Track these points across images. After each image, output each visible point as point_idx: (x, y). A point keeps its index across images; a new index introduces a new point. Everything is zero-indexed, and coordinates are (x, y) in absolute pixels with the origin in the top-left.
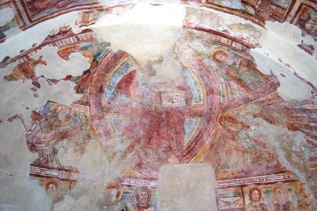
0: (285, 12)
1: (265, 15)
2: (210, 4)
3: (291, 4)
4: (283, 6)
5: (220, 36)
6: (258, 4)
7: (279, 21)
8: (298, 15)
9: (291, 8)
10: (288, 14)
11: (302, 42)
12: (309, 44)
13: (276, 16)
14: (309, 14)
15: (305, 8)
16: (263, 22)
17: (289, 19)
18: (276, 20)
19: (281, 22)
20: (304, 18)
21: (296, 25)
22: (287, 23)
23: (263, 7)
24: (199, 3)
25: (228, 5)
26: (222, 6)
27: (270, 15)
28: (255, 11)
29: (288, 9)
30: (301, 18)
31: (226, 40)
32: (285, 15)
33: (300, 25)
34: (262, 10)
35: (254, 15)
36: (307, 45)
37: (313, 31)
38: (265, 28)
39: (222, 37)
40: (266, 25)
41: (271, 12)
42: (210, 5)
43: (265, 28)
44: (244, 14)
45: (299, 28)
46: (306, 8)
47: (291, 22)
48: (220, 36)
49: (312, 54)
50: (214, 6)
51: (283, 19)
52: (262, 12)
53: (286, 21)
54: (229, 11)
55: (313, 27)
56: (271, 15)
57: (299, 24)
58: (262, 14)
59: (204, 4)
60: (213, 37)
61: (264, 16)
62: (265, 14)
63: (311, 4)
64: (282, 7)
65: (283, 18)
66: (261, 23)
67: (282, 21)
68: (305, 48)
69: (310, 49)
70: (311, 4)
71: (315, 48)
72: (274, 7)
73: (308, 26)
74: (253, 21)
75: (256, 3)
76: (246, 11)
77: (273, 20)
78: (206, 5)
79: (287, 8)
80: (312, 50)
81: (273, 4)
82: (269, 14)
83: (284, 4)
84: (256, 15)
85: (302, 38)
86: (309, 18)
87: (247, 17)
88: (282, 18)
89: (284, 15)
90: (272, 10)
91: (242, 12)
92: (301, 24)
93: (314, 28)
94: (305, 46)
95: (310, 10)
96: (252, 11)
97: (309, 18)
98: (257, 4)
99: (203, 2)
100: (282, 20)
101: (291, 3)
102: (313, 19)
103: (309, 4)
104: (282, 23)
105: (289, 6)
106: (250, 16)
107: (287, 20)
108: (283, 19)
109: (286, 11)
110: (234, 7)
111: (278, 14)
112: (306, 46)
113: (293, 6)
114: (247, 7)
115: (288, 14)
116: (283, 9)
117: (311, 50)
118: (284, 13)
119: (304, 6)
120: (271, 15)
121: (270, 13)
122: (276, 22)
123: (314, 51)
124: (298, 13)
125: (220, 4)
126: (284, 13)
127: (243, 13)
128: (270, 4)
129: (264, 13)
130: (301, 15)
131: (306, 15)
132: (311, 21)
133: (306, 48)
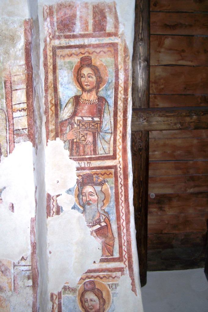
0: (91, 155)
1: (69, 133)
2: (51, 54)
3: (107, 156)
4: (99, 148)
5: (25, 87)
6: (84, 118)
7: (71, 155)
8: (95, 171)
9: (102, 158)
10: (91, 159)
11: (57, 196)
12: (59, 205)
13: (78, 147)
14: (104, 181)
15: (111, 173)
16: (57, 135)
17: (83, 164)
18: (71, 150)
19: (72, 157)
20: (94, 179)
21: (78, 176)
22: (75, 164)
23: (81, 125)
24: (51, 37)
25: (62, 79)
26: (57, 71)
27: (73, 140)
28: (68, 119)
29: (97, 156)
30: (93, 176)
31: (24, 98)
32: (87, 157)
33: (83, 180)
34: (76, 126)
35: (59, 120)
36: (57, 204)
37: (84, 198)
38: (47, 142)
39: (25, 91)
40: (54, 141)
41: (79, 140)
42: (50, 53)
43: (47, 142)
44: (54, 107)
45: (76, 181)
46: (112, 174)
47: (78, 169)
48: (27, 87)
49: (50, 216)
50: (51, 61)
51: (77, 157)
52: (72, 128)
53: (77, 162)
54: (49, 84)
55: (91, 195)
56: (75, 141)
57: (83, 178)
58: (68, 128)
59: (50, 44)
60: (19, 77)
61: (66, 133)
62: (71, 132)
63: (120, 176)
64: (95, 147)
65: (80, 157)
66: (52, 134)
67: (74, 158)
68: (51, 204)
69: (54, 210)
70: (120, 176)
71: (61, 214)
72: (90, 139)
73: (89, 189)
74: (47, 122)
75: (83, 115)
76: (61, 108)
77: (67, 147)
78: (48, 47)
79: (98, 154)
80: (54, 214)
81: (94, 137)
82: (74, 138)
83: (102, 149)
84: (62, 123)
85: (63, 192)
86: (101, 184)
87: (50, 113)
88: (79, 155)
89: (85, 155)
90: (83, 138)
91: (55, 102)
92: (84, 181)
93: (90, 197)
94: (53, 202)
95: (112, 179)
96: (65, 114)
97: (101, 184)
98: (82, 117)
99: (53, 41)
100: (75, 157)
101: (108, 155)
102: (103, 189)
103: (119, 175)
104: (70, 158)
105: (103, 155)
106: (54, 115)
107: (80, 162)
108: (77, 157)
109: (94, 155)
110: (60, 89)
111: (81, 148)
112: (55, 204)
113: (106, 160)
114: (70, 106)
115: (91, 159)
116: (95, 151)
117: (54, 212)
118: (89, 154)
119: (113, 170)
120: (75, 141)
121: (78, 138)
122: (67, 152)
123: (55, 216)
124: (98, 169)
125: (58, 67)
126: (89, 154)
127: (55, 104)
128: (93, 132)
129: (73, 130)
130: (97, 174)
131: (101, 178)
132: (98, 188)
133: (52, 206)
